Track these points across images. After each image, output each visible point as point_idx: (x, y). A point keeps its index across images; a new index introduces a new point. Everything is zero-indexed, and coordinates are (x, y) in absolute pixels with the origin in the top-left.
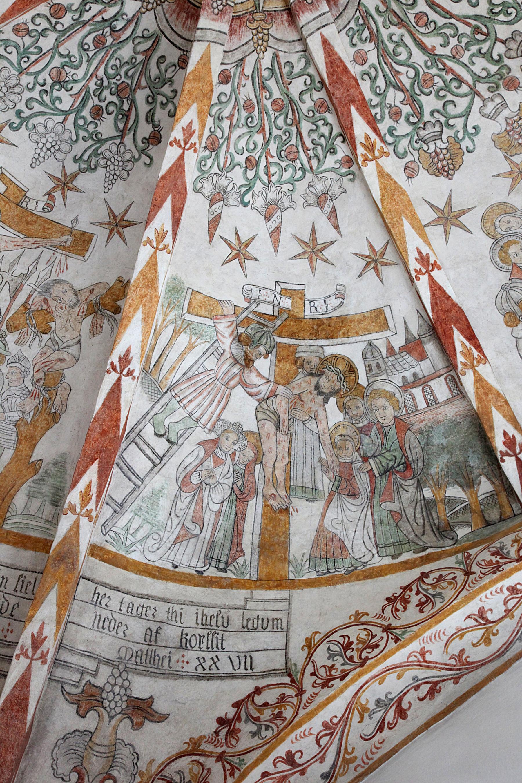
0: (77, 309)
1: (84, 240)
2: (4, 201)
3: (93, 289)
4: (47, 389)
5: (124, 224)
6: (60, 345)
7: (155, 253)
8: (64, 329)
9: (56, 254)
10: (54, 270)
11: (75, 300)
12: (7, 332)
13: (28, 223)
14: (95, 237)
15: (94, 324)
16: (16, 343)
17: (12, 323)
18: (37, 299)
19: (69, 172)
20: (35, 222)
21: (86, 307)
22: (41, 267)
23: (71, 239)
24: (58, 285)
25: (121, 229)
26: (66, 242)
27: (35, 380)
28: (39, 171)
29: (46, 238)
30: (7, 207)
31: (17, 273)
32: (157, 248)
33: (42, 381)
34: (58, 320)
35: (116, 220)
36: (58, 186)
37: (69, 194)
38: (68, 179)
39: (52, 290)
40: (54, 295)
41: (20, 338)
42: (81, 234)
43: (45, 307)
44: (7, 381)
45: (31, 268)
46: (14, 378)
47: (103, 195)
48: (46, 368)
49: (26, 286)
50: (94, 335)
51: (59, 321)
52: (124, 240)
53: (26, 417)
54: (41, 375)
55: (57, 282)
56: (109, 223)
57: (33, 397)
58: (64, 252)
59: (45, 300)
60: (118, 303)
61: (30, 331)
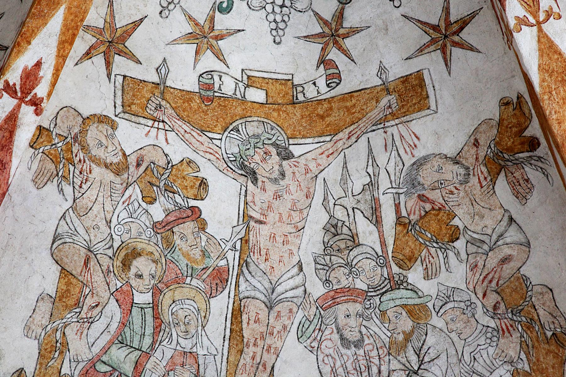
0: (474, 181)
1: (413, 86)
2: (274, 110)
3: (476, 140)
4: (516, 311)
5: (455, 28)
6: (487, 241)
7: (540, 30)
8: (477, 217)
9: (389, 130)
10: (402, 152)
11: (462, 171)
12: (404, 272)
13: (322, 117)
14: (426, 73)
15: (514, 185)
16: (427, 277)
17: (401, 257)
18: (410, 204)
19: (327, 15)
20: (331, 109)
21: (484, 169)
22: (382, 159)
23: (393, 98)
24: (424, 167)
25: (456, 38)
26: (390, 107)
27: (491, 309)
28: (289, 41)
29: (360, 119)
30: (283, 115)
31: (358, 188)
32: (539, 23)
33: (502, 306)
34: (459, 212)
35: (439, 31)
36: (326, 44)
37: (348, 43)
38: (333, 26)
39: (421, 179)
40: (427, 183)
41: (427, 268)
42: (403, 82)
43: (428, 207)
44: (453, 335)
45: (370, 170)
46: (460, 325)
47: (397, 13)
48: (494, 284)
49: (381, 197)
50: (525, 197)
51: (461, 211)
52: (471, 48)
53: (520, 366)
54: (493, 298)
55: (419, 164)
56: (433, 41)
57: (507, 334)
58: (397, 121)
59: (422, 198)
60: (527, 133)
61: (433, 250)
